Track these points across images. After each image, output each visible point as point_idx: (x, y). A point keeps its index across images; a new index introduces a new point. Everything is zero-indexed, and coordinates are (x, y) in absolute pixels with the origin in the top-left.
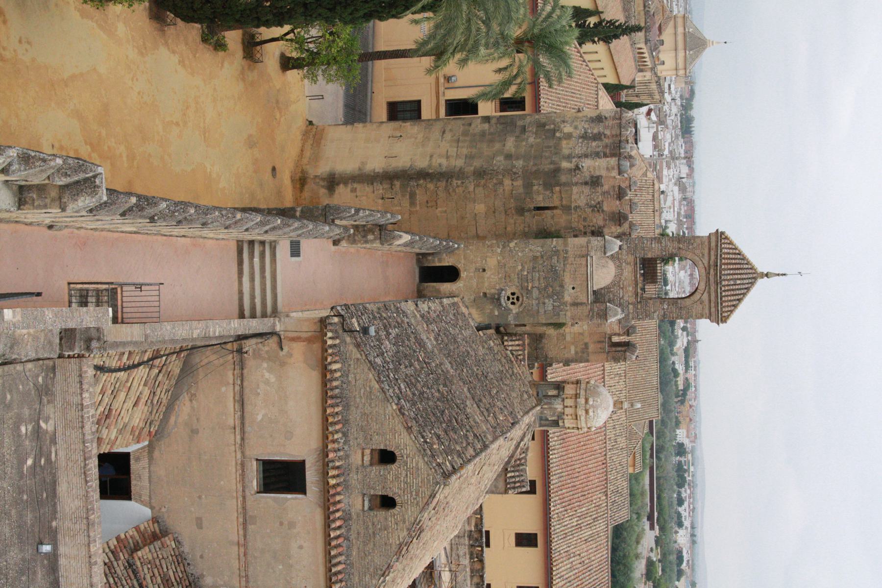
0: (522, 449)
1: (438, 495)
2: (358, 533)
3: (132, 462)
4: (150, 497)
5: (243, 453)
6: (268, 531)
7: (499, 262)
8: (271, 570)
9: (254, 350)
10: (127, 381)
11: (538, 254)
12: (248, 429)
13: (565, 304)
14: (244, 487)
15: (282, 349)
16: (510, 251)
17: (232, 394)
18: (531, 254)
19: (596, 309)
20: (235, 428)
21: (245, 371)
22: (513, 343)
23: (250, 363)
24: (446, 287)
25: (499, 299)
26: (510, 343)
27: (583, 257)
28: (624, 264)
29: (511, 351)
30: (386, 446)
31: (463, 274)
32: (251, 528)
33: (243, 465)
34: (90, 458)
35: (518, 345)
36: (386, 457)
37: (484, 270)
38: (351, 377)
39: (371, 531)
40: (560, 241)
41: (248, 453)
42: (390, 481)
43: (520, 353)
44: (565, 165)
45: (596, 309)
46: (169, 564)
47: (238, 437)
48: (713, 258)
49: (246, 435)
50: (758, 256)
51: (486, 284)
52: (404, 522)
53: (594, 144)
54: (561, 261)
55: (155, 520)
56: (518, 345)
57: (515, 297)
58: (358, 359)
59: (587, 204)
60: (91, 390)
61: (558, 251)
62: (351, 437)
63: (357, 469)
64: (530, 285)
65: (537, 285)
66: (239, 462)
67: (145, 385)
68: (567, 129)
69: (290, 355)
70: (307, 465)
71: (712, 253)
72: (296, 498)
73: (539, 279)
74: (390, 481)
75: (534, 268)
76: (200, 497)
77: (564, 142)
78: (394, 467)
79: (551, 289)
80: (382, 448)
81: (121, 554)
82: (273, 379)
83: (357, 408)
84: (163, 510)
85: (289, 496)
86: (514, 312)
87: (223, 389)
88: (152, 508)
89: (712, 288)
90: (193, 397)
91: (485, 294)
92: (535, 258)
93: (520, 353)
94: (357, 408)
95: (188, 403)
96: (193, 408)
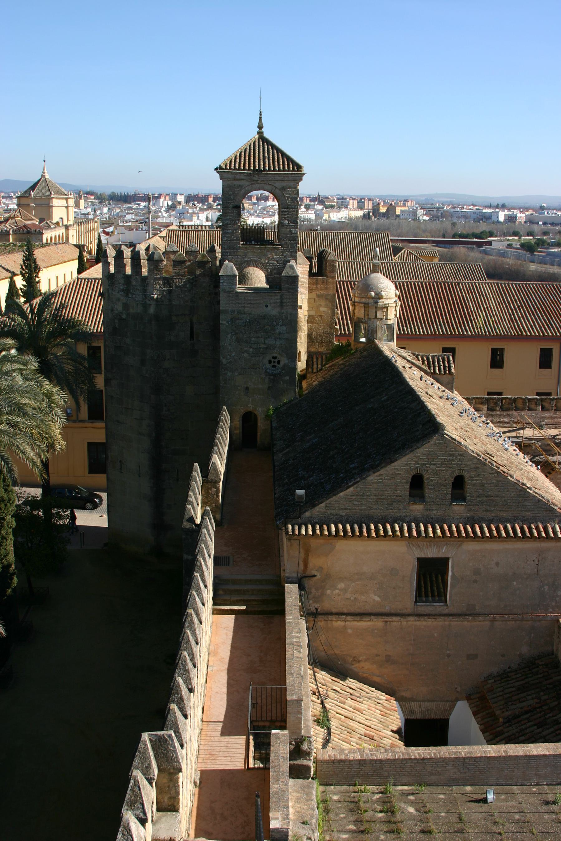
0: (413, 359)
1: (454, 437)
2: (487, 511)
3: (414, 717)
4: (447, 701)
5: (409, 615)
6: (481, 593)
8: (518, 592)
9: (315, 602)
10: (340, 719)
12: (387, 609)
14: (440, 615)
15: (314, 576)
17: (356, 623)
19: (287, 286)
20: (386, 622)
21: (334, 611)
22: (315, 363)
23: (326, 605)
24: (261, 424)
25: (275, 375)
26: (315, 366)
28: (246, 259)
29: (322, 366)
30: (406, 483)
31: (251, 407)
32: (478, 609)
33: (419, 615)
34: (409, 754)
35: (317, 359)
36: (417, 483)
37: (247, 388)
38: (342, 513)
39: (485, 499)
40: (222, 316)
41: (409, 611)
42: (438, 480)
43: (324, 357)
44: (152, 310)
45: (287, 286)
46: (509, 686)
47: (394, 618)
49: (393, 611)
50: (243, 136)
51: (261, 386)
52: (478, 468)
53: (134, 283)
55: (468, 698)
56: (317, 359)
57: (273, 360)
58: (326, 506)
60: (346, 752)
61: (232, 319)
62: (398, 515)
63: (427, 510)
65: (263, 340)
66: (417, 618)
67: (344, 703)
68: (119, 307)
69: (320, 569)
70: (423, 556)
72: (452, 567)
73: (257, 337)
74: (438, 480)
76: (449, 656)
77: (131, 311)
78: (426, 477)
79: (268, 327)
80: (408, 486)
81: (498, 729)
82: (341, 585)
83: (371, 508)
84: (459, 689)
85: (450, 573)
86: (287, 361)
87: (350, 631)
88: (457, 700)
90: (356, 660)
91: (269, 388)
93: (324, 357)
94: (371, 508)
95: (362, 664)
96: (366, 660)
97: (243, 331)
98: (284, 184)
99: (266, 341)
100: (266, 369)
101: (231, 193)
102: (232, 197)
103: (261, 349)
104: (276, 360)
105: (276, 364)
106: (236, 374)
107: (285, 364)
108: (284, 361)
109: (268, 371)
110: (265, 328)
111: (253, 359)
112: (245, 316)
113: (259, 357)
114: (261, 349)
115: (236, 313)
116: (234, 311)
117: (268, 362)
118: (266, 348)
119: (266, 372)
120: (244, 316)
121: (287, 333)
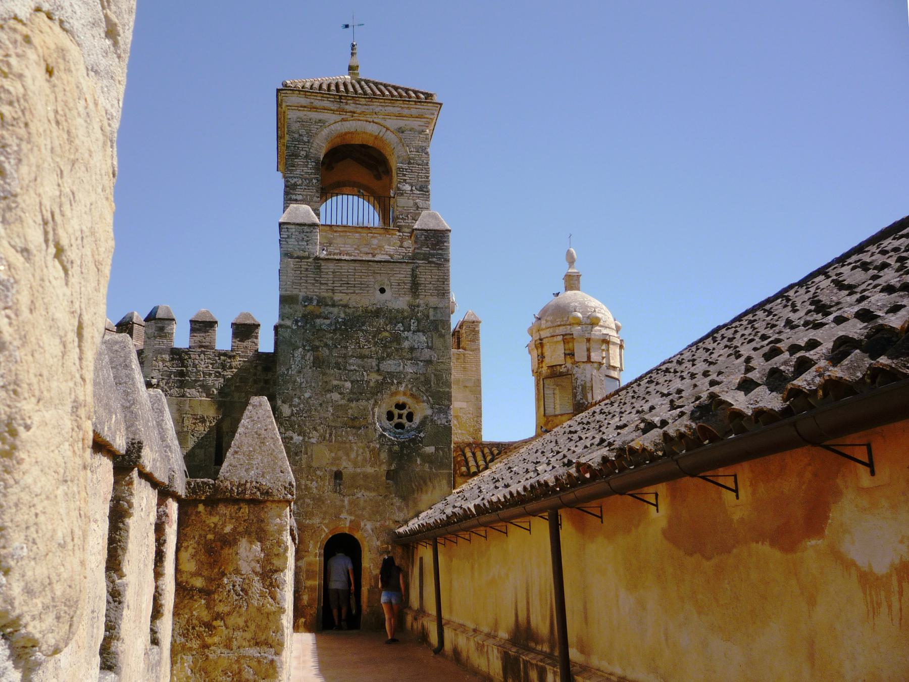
11: (309, 356)
13: (412, 307)
18: (308, 371)
26: (472, 463)
37: (338, 475)
48: (326, 104)
51: (370, 470)
54: (325, 310)
57: (396, 412)
61: (304, 316)
71: (317, 103)
75: (338, 366)
86: (429, 412)
89: (377, 110)
91: (389, 475)
92: (318, 363)
97: (330, 343)
98: (401, 123)
101: (303, 132)
102: (305, 139)
105: (404, 420)
107: (426, 418)
108: (422, 410)
111: (354, 404)
112: (335, 310)
115: (315, 302)
116: (309, 299)
117: (385, 416)
120: (331, 309)
121: (428, 347)
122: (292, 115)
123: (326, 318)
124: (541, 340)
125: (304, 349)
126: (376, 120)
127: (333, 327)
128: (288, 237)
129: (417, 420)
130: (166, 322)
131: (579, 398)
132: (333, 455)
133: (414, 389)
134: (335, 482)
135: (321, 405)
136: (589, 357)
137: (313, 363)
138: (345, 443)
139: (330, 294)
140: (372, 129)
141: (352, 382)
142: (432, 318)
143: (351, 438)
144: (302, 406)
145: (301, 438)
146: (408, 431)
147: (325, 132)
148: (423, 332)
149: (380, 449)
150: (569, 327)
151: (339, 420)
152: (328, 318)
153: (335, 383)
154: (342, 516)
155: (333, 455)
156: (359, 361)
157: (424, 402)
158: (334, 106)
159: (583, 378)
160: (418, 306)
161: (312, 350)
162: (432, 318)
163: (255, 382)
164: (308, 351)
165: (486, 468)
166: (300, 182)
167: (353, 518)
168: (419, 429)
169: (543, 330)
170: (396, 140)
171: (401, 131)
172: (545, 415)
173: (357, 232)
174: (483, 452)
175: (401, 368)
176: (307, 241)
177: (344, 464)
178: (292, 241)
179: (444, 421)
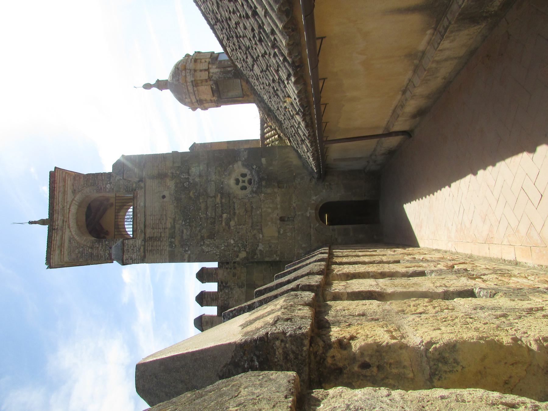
7: (261, 231)
11: (207, 242)
16: (244, 246)
27: (151, 238)
31: (311, 212)
37: (282, 219)
51: (279, 199)
57: (241, 184)
59: (231, 289)
61: (182, 246)
64: (218, 200)
65: (210, 200)
75: (213, 223)
86: (240, 163)
92: (212, 236)
97: (198, 229)
98: (69, 191)
99: (212, 194)
100: (252, 192)
103: (223, 201)
104: (241, 179)
105: (246, 179)
106: (261, 236)
107: (243, 165)
109: (254, 189)
110: (193, 196)
111: (237, 212)
112: (177, 226)
113: (234, 203)
114: (223, 201)
115: (173, 240)
118: (222, 194)
119: (256, 192)
122: (66, 259)
123: (183, 232)
124: (197, 101)
125: (203, 245)
126: (68, 207)
127: (189, 227)
128: (131, 259)
129: (245, 171)
130: (203, 320)
131: (231, 76)
132: (270, 223)
133: (226, 173)
134: (287, 221)
135: (238, 233)
136: (205, 70)
137: (211, 239)
138: (261, 215)
139: (167, 230)
140: (73, 209)
141: (223, 213)
142: (180, 165)
143: (258, 212)
144: (240, 245)
145: (260, 244)
146: (253, 176)
147: (77, 238)
148: (189, 170)
149: (265, 194)
150: (188, 84)
151: (247, 220)
152: (183, 231)
153: (224, 224)
154: (308, 215)
155: (270, 223)
156: (210, 210)
157: (233, 167)
158: (60, 233)
159: (218, 73)
160: (172, 173)
161: (203, 240)
162: (180, 165)
163: (235, 268)
164: (204, 242)
165: (276, 130)
166: (108, 251)
167: (309, 208)
168: (251, 169)
169: (191, 101)
170: (80, 193)
171: (74, 192)
172: (243, 97)
173: (137, 215)
174: (266, 133)
175: (213, 182)
176: (134, 247)
177: (275, 215)
178: (134, 256)
179: (246, 153)
